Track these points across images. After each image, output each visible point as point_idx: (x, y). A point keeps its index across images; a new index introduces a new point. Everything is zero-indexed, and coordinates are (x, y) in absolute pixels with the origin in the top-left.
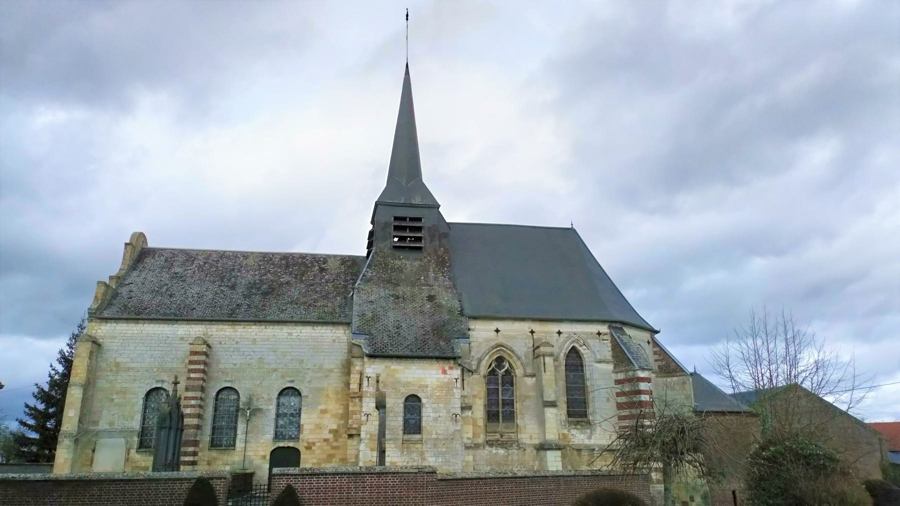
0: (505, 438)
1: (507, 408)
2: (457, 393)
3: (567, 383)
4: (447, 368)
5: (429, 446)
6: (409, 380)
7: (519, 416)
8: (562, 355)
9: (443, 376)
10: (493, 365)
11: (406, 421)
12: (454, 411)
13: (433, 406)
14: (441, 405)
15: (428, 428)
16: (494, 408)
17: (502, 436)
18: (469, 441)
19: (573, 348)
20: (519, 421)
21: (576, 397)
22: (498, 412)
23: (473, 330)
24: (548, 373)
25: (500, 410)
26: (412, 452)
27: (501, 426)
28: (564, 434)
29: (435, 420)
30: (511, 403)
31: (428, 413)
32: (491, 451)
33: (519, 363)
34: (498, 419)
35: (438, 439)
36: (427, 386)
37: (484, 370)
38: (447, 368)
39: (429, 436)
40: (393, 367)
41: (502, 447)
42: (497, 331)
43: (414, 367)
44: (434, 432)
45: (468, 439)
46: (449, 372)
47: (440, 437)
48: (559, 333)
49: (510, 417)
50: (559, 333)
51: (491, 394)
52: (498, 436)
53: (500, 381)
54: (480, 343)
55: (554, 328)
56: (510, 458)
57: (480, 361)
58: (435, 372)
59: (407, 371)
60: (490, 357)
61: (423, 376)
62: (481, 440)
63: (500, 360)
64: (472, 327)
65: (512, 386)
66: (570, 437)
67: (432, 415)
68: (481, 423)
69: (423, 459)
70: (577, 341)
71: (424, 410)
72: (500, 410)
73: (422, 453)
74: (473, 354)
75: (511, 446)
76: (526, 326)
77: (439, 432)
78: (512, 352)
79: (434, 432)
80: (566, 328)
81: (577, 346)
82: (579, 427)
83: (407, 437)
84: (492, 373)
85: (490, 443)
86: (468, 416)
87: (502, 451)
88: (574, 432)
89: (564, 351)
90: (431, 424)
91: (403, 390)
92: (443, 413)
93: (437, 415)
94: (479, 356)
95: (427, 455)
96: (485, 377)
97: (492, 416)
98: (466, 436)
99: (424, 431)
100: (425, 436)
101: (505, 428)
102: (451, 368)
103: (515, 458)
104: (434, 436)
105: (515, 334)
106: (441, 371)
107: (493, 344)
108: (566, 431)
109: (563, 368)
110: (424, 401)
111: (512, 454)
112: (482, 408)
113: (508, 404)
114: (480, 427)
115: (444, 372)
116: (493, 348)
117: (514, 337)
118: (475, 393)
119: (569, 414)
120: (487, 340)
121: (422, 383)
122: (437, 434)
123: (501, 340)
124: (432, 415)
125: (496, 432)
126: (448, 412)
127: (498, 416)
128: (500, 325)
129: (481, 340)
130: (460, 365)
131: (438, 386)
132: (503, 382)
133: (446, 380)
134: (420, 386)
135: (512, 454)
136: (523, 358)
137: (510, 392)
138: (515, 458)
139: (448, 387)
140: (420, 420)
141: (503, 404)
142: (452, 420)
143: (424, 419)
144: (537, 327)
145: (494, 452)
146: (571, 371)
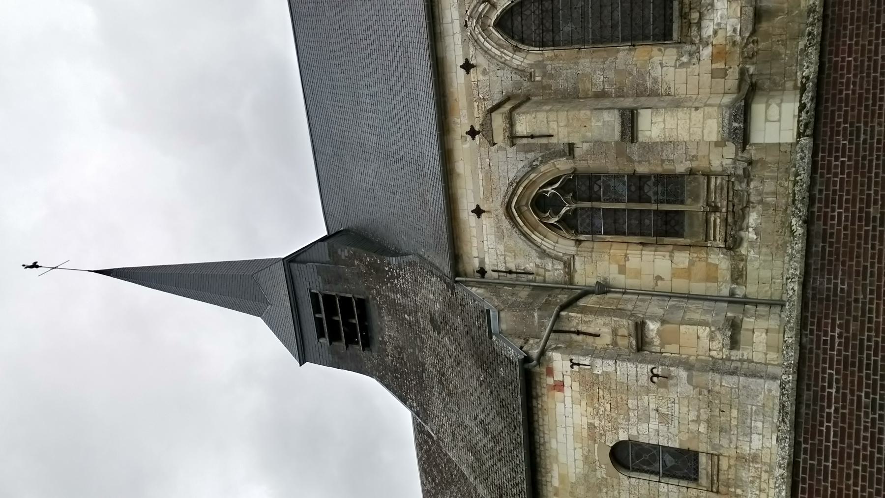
0: (722, 204)
1: (650, 190)
2: (602, 367)
3: (583, 42)
4: (550, 381)
5: (725, 442)
6: (579, 454)
7: (667, 167)
8: (518, 60)
9: (567, 392)
10: (553, 221)
11: (670, 473)
12: (644, 380)
13: (633, 420)
14: (632, 403)
15: (685, 437)
16: (650, 221)
17: (716, 209)
18: (719, 336)
19: (498, 25)
20: (681, 168)
21: (618, 15)
22: (657, 212)
23: (482, 261)
24: (553, 128)
25: (656, 205)
26: (737, 478)
27: (694, 207)
28: (714, 58)
29: (664, 418)
30: (638, 181)
31: (649, 432)
32: (752, 243)
33: (543, 168)
34: (677, 212)
35: (708, 421)
36: (591, 426)
37: (564, 245)
38: (550, 381)
39: (703, 438)
40: (556, 483)
41: (744, 217)
42: (478, 212)
43: (553, 444)
44: (693, 427)
45: (712, 338)
46: (558, 377)
47: (704, 417)
48: (467, 66)
49: (672, 185)
50: (467, 66)
51: (617, 226)
52: (716, 219)
53: (587, 205)
54: (507, 249)
55: (458, 79)
56: (770, 199)
57: (544, 254)
58: (560, 407)
59: (562, 459)
60: (534, 229)
61: (570, 431)
62: (721, 262)
63: (541, 204)
64: (476, 264)
65: (598, 177)
66: (720, 40)
67: (654, 424)
68: (683, 258)
69: (755, 458)
70: (482, 19)
71: (643, 439)
72: (656, 205)
73: (742, 459)
74: (530, 267)
75: (736, 193)
76: (465, 151)
77: (693, 416)
78: (518, 184)
79: (693, 427)
80: (456, 50)
81: (494, 17)
82: (695, 16)
83: (704, 481)
84: (569, 225)
85: (732, 244)
86: (659, 333)
87: (753, 218)
88: (708, 30)
89: (508, 55)
90: (674, 430)
91: (601, 473)
92: (650, 401)
93: (653, 414)
94: (534, 254)
95: (745, 449)
96: (579, 242)
97: (666, 228)
98: (705, 342)
99: (693, 447)
100: (702, 447)
101: (696, 199)
102: (550, 372)
103: (770, 186)
104: (703, 428)
105: (483, 174)
106: (558, 395)
107: (506, 224)
108: (706, 52)
109: (548, 53)
110: (623, 436)
111: (760, 194)
112: (648, 254)
113: (641, 188)
114: (692, 263)
115: (559, 386)
116: (515, 224)
117: (488, 175)
118: (614, 268)
119: (663, 36)
120: (500, 235)
121: (585, 433)
122: (697, 421)
123: (496, 205)
124: (654, 424)
125: (707, 221)
126: (648, 391)
127: (667, 212)
128: (467, 203)
129: (501, 248)
130: (543, 353)
131: (591, 403)
132: (590, 200)
133: (576, 385)
134: (592, 438)
135: (760, 194)
136: (531, 156)
137: (612, 183)
138: (770, 186)
139: (591, 385)
140: (666, 449)
141: (640, 200)
142: (665, 386)
143: (663, 442)
144: (462, 122)
145: (752, 235)
146: (555, 30)
